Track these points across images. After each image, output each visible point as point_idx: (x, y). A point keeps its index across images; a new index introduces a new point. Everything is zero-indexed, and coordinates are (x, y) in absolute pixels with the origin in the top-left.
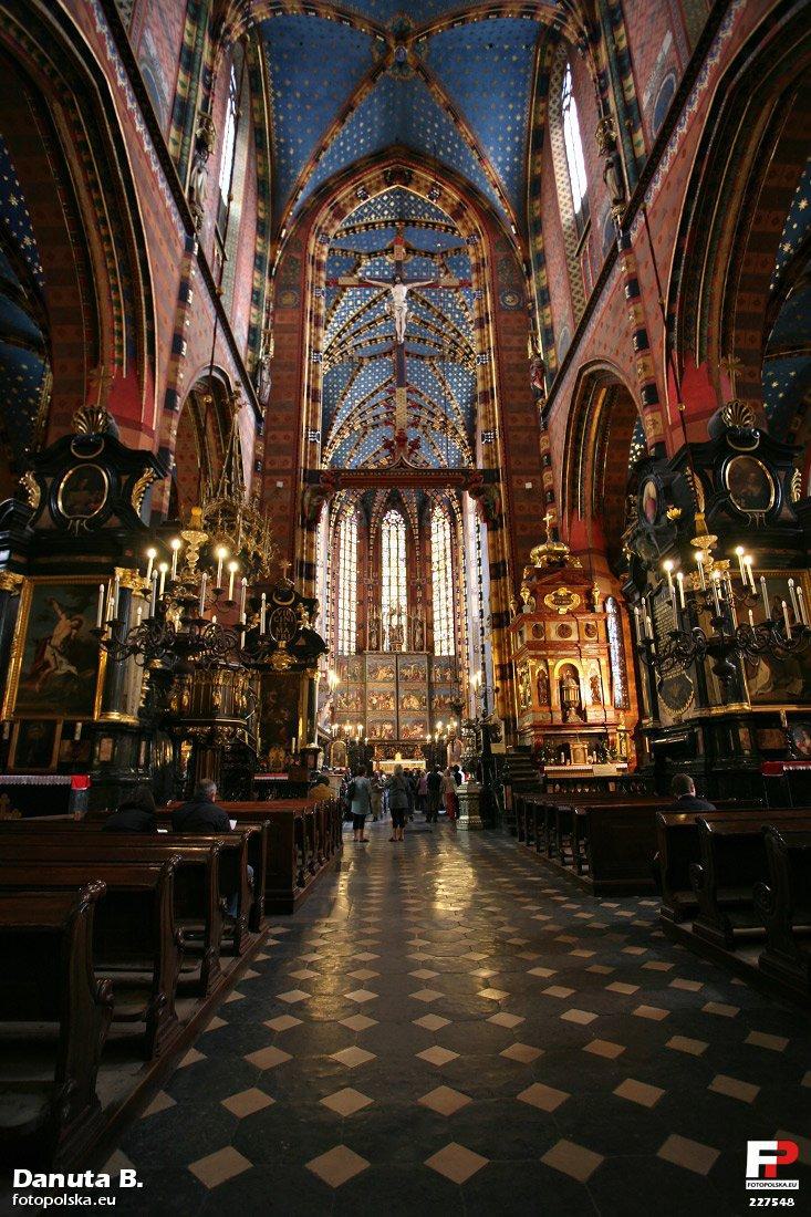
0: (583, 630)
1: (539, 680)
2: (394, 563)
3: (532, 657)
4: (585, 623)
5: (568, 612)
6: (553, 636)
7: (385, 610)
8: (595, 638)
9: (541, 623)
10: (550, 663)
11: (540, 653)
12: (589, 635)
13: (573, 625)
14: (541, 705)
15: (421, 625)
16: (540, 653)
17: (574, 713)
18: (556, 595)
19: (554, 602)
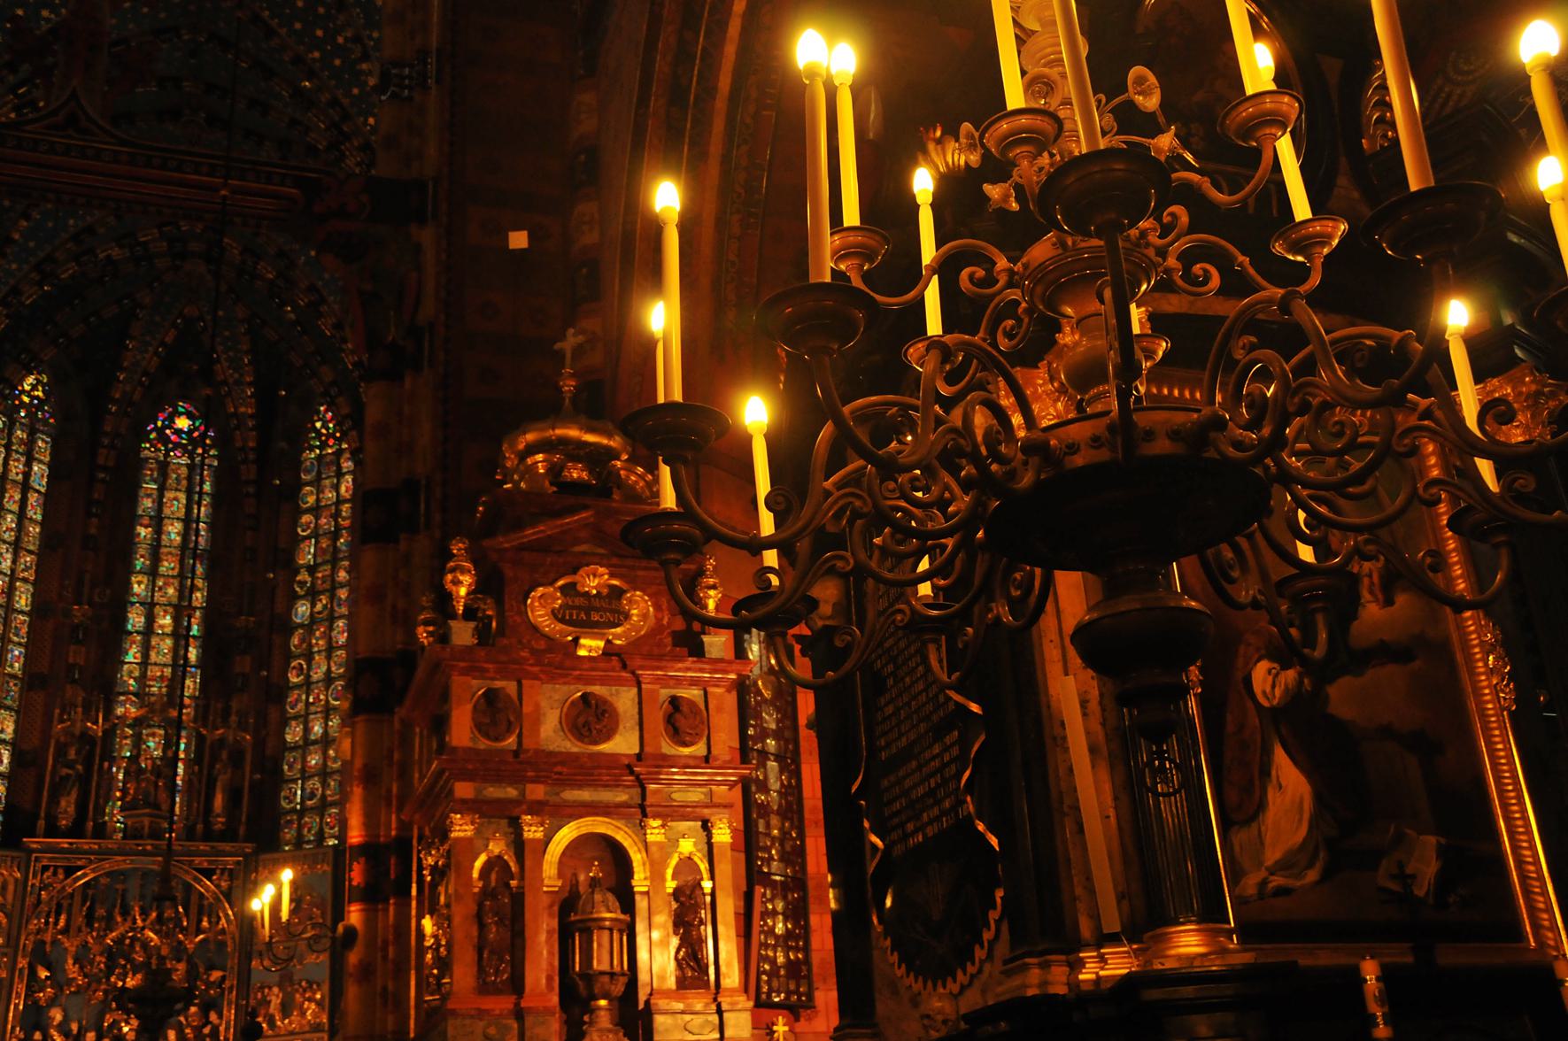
0: (656, 719)
1: (486, 893)
2: (168, 566)
3: (467, 807)
4: (665, 693)
5: (609, 652)
6: (550, 732)
7: (127, 709)
8: (699, 749)
9: (510, 687)
10: (532, 832)
11: (493, 792)
12: (678, 737)
13: (624, 700)
14: (484, 988)
15: (237, 758)
16: (493, 792)
17: (604, 1020)
18: (569, 590)
19: (556, 615)
